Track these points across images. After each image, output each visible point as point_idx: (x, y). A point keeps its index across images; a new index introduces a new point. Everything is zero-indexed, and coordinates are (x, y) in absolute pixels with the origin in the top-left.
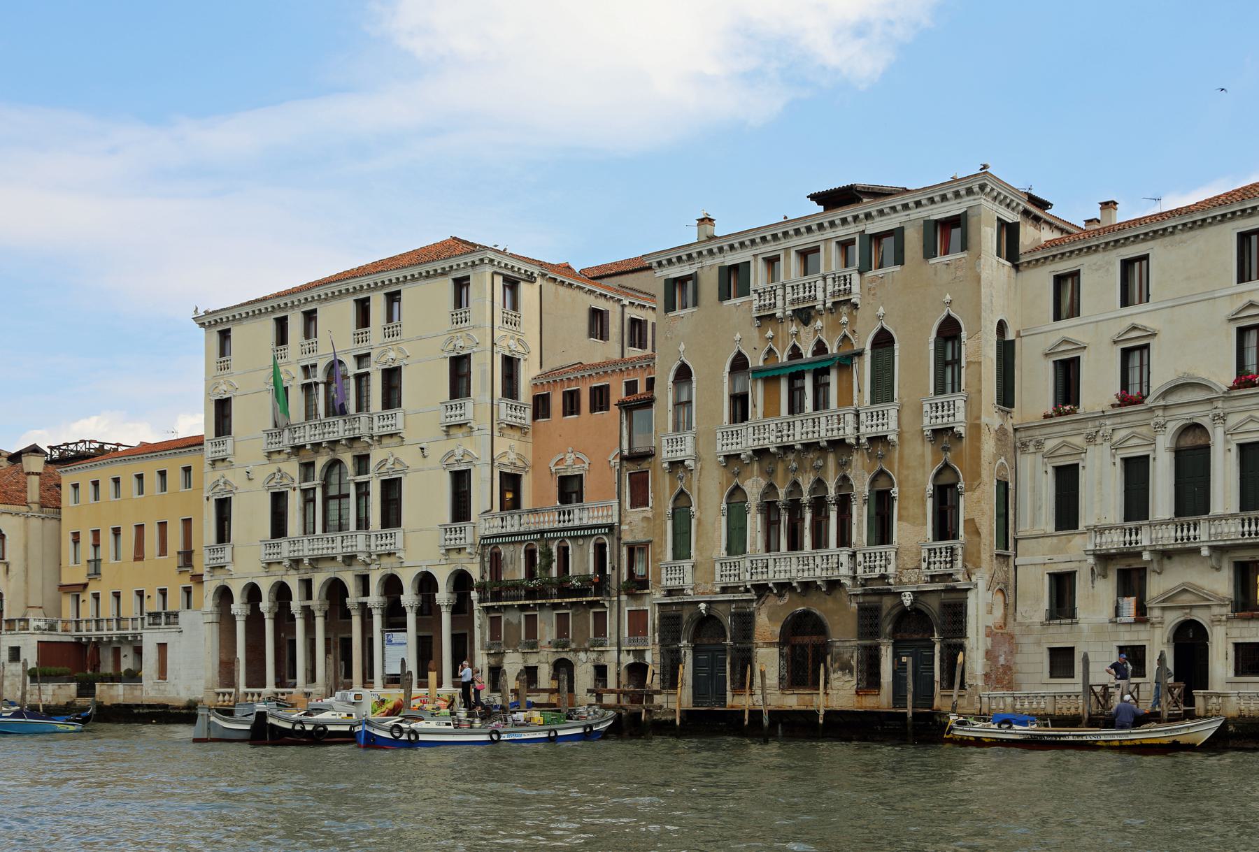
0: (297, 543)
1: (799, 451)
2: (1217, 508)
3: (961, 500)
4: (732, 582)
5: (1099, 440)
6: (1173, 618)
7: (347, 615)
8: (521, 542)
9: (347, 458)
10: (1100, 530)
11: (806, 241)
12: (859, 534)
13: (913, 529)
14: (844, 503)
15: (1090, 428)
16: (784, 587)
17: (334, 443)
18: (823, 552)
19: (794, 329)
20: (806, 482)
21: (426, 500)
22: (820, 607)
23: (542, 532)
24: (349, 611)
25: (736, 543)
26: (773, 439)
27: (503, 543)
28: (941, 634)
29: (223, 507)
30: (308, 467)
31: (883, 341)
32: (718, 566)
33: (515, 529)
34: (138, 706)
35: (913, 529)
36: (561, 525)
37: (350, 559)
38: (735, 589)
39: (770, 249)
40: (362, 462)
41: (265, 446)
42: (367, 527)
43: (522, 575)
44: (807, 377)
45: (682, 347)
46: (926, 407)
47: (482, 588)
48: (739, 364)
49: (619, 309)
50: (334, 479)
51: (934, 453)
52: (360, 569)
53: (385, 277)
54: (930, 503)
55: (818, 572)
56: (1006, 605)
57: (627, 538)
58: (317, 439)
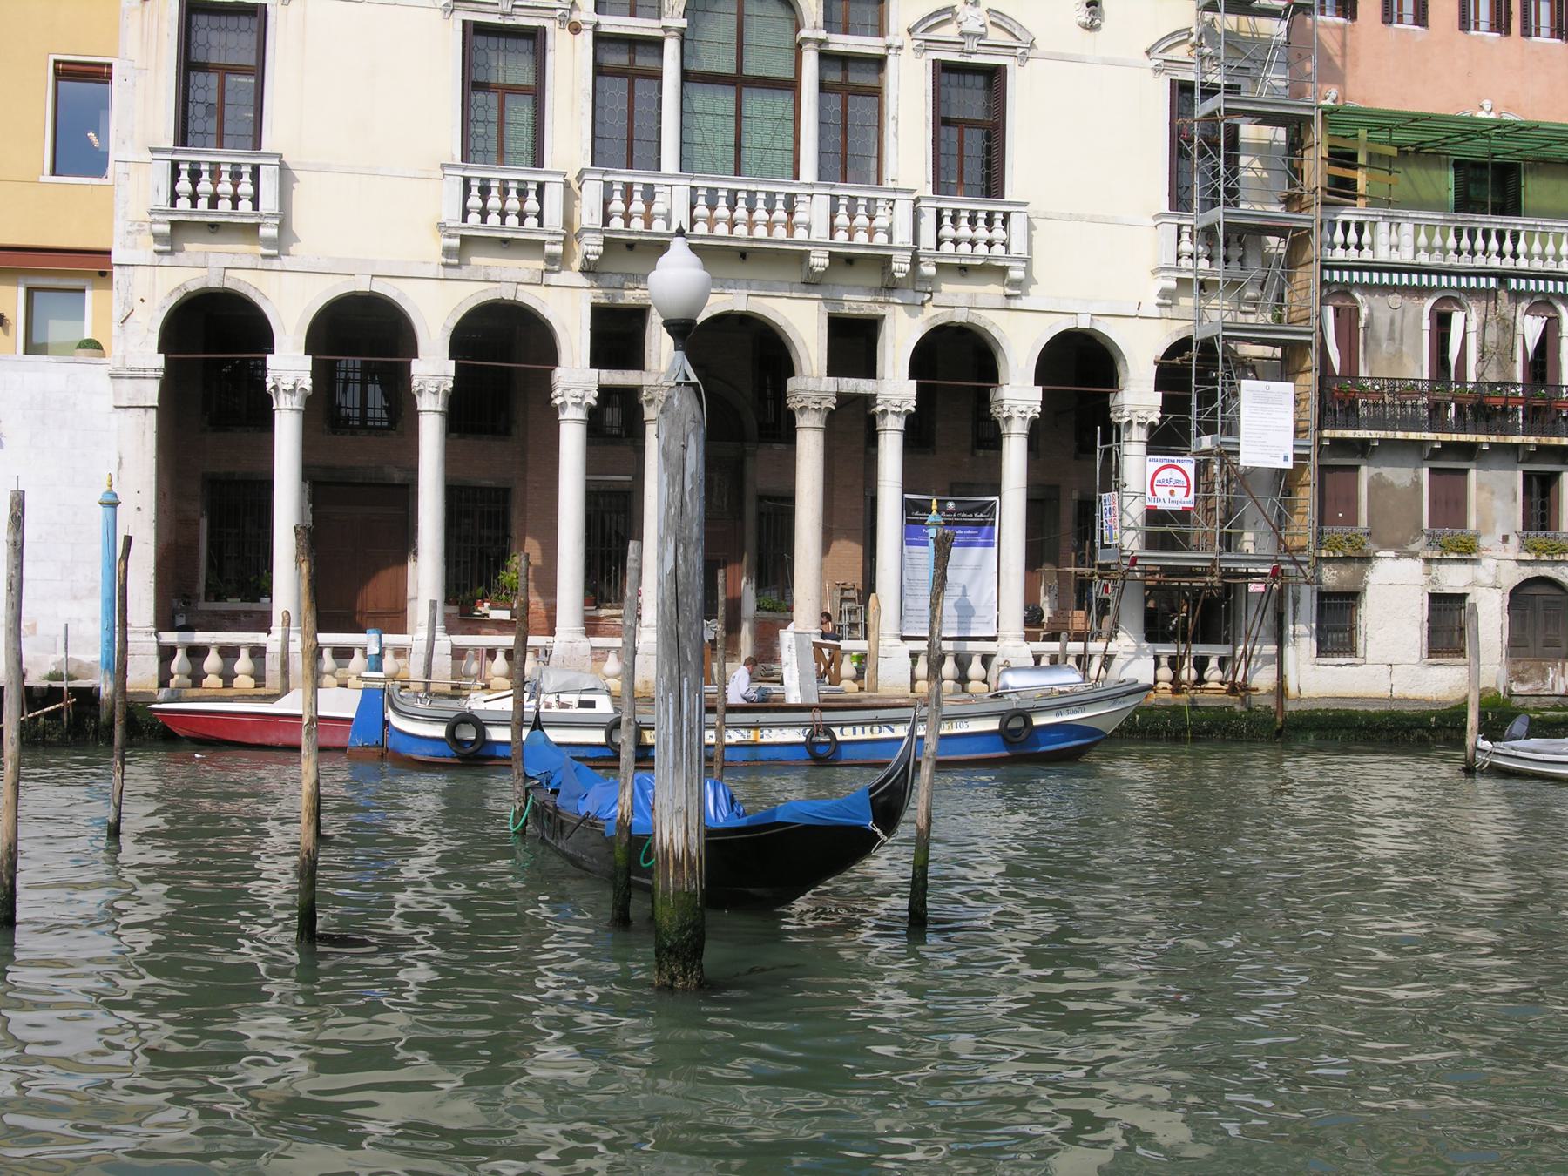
23: (1503, 277)
24: (791, 417)
33: (1405, 256)
36: (1465, 261)
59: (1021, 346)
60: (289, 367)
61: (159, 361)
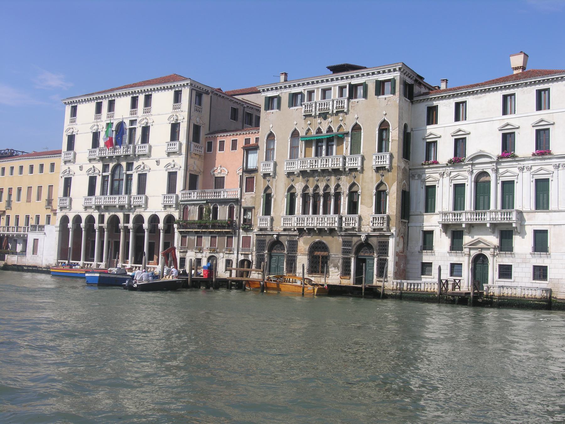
0: (99, 199)
1: (319, 172)
2: (492, 207)
3: (388, 197)
4: (288, 226)
5: (445, 175)
6: (474, 253)
7: (118, 231)
8: (197, 204)
9: (124, 164)
10: (445, 214)
11: (325, 85)
12: (344, 209)
13: (366, 209)
14: (338, 196)
15: (441, 170)
16: (311, 231)
17: (118, 157)
18: (328, 216)
19: (319, 121)
20: (322, 186)
21: (157, 185)
22: (326, 239)
25: (291, 211)
26: (309, 166)
27: (189, 204)
28: (378, 253)
29: (68, 182)
30: (105, 167)
31: (357, 128)
32: (282, 219)
33: (195, 198)
34: (25, 266)
35: (366, 209)
37: (122, 208)
38: (289, 230)
39: (310, 87)
40: (130, 166)
41: (88, 156)
42: (130, 193)
43: (196, 218)
44: (325, 142)
45: (271, 126)
46: (374, 157)
47: (178, 223)
48: (295, 134)
49: (242, 108)
50: (117, 172)
51: (377, 177)
53: (146, 88)
54: (374, 197)
55: (326, 225)
56: (404, 243)
57: (244, 205)
58: (111, 155)
59: (146, 217)
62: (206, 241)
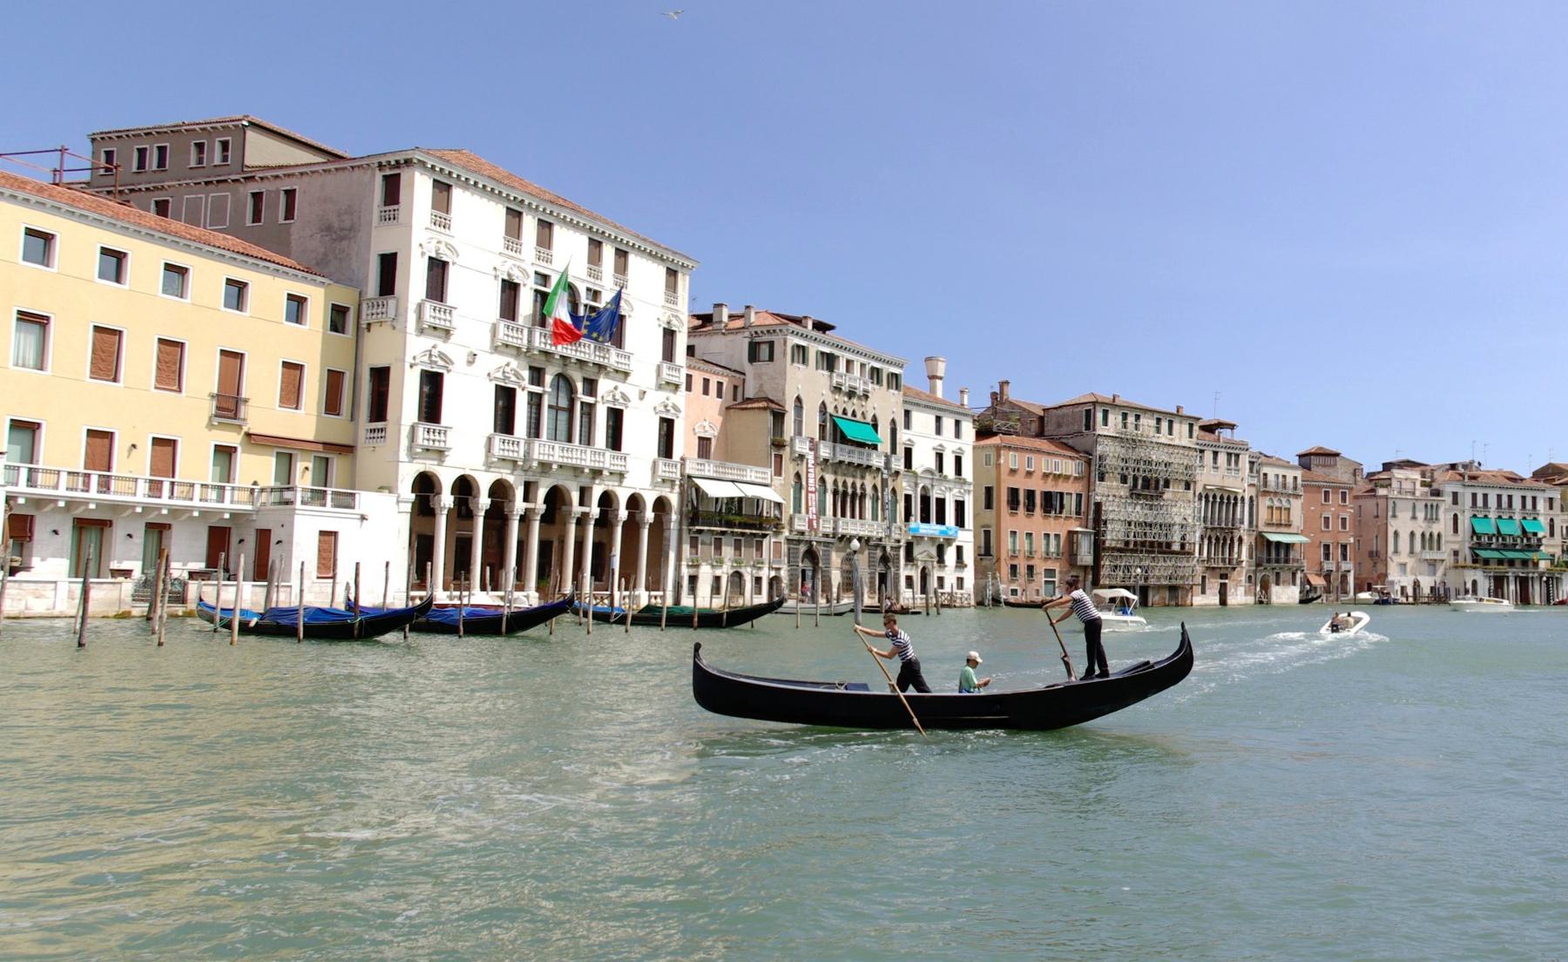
21: (640, 434)
30: (537, 375)
37: (577, 470)
40: (591, 387)
52: (585, 482)
59: (623, 496)
60: (447, 499)
61: (413, 496)
62: (728, 551)
